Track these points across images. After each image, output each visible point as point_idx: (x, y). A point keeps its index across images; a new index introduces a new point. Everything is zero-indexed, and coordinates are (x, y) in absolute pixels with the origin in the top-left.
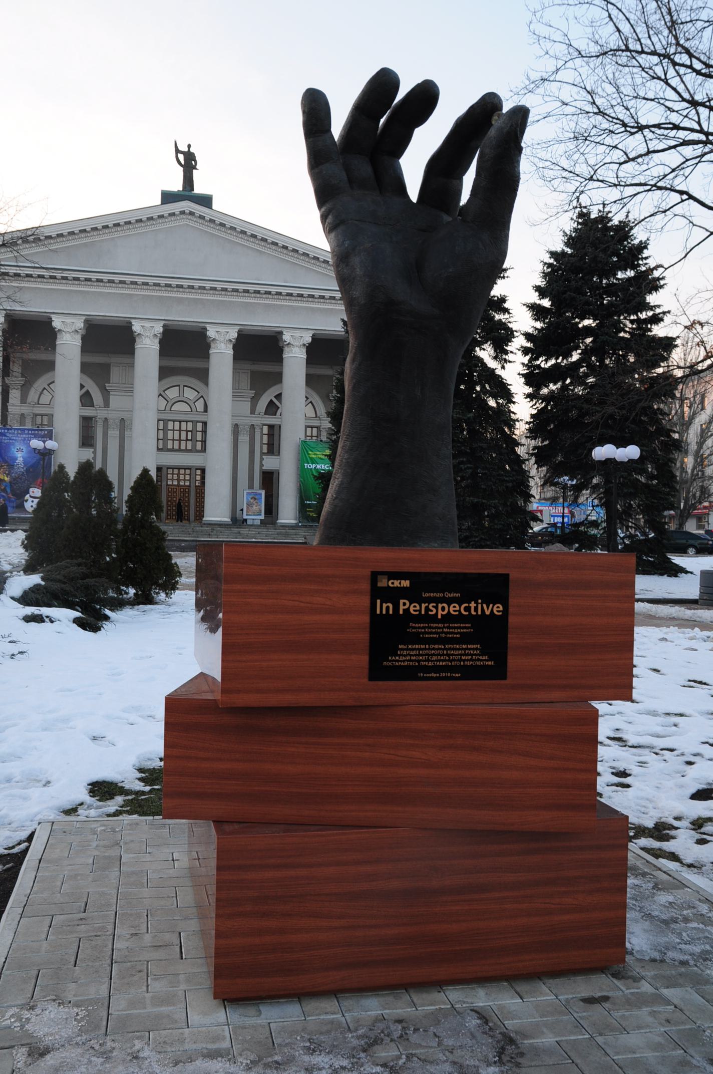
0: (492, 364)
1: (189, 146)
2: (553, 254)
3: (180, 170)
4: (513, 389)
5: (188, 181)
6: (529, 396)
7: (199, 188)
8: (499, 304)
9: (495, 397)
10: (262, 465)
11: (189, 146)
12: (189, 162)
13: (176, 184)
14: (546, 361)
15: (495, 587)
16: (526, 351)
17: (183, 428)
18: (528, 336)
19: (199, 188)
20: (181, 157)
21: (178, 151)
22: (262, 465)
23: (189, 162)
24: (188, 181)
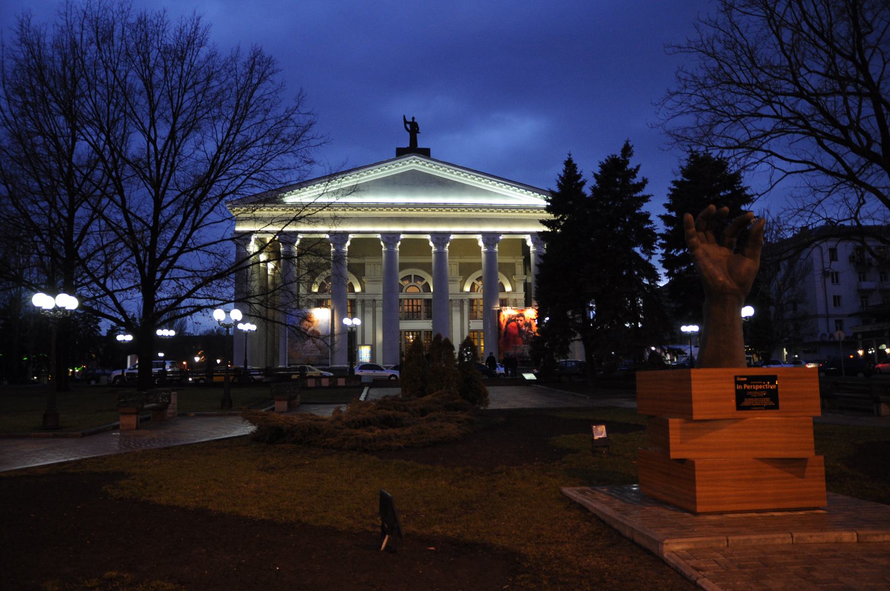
0: (645, 257)
1: (413, 118)
2: (675, 183)
3: (408, 135)
4: (658, 272)
5: (413, 141)
6: (666, 275)
7: (421, 145)
8: (645, 217)
9: (648, 278)
10: (469, 327)
11: (413, 118)
13: (406, 144)
14: (677, 251)
15: (772, 379)
16: (662, 246)
17: (415, 303)
18: (663, 236)
19: (421, 145)
20: (408, 126)
21: (406, 122)
22: (469, 327)
24: (413, 141)
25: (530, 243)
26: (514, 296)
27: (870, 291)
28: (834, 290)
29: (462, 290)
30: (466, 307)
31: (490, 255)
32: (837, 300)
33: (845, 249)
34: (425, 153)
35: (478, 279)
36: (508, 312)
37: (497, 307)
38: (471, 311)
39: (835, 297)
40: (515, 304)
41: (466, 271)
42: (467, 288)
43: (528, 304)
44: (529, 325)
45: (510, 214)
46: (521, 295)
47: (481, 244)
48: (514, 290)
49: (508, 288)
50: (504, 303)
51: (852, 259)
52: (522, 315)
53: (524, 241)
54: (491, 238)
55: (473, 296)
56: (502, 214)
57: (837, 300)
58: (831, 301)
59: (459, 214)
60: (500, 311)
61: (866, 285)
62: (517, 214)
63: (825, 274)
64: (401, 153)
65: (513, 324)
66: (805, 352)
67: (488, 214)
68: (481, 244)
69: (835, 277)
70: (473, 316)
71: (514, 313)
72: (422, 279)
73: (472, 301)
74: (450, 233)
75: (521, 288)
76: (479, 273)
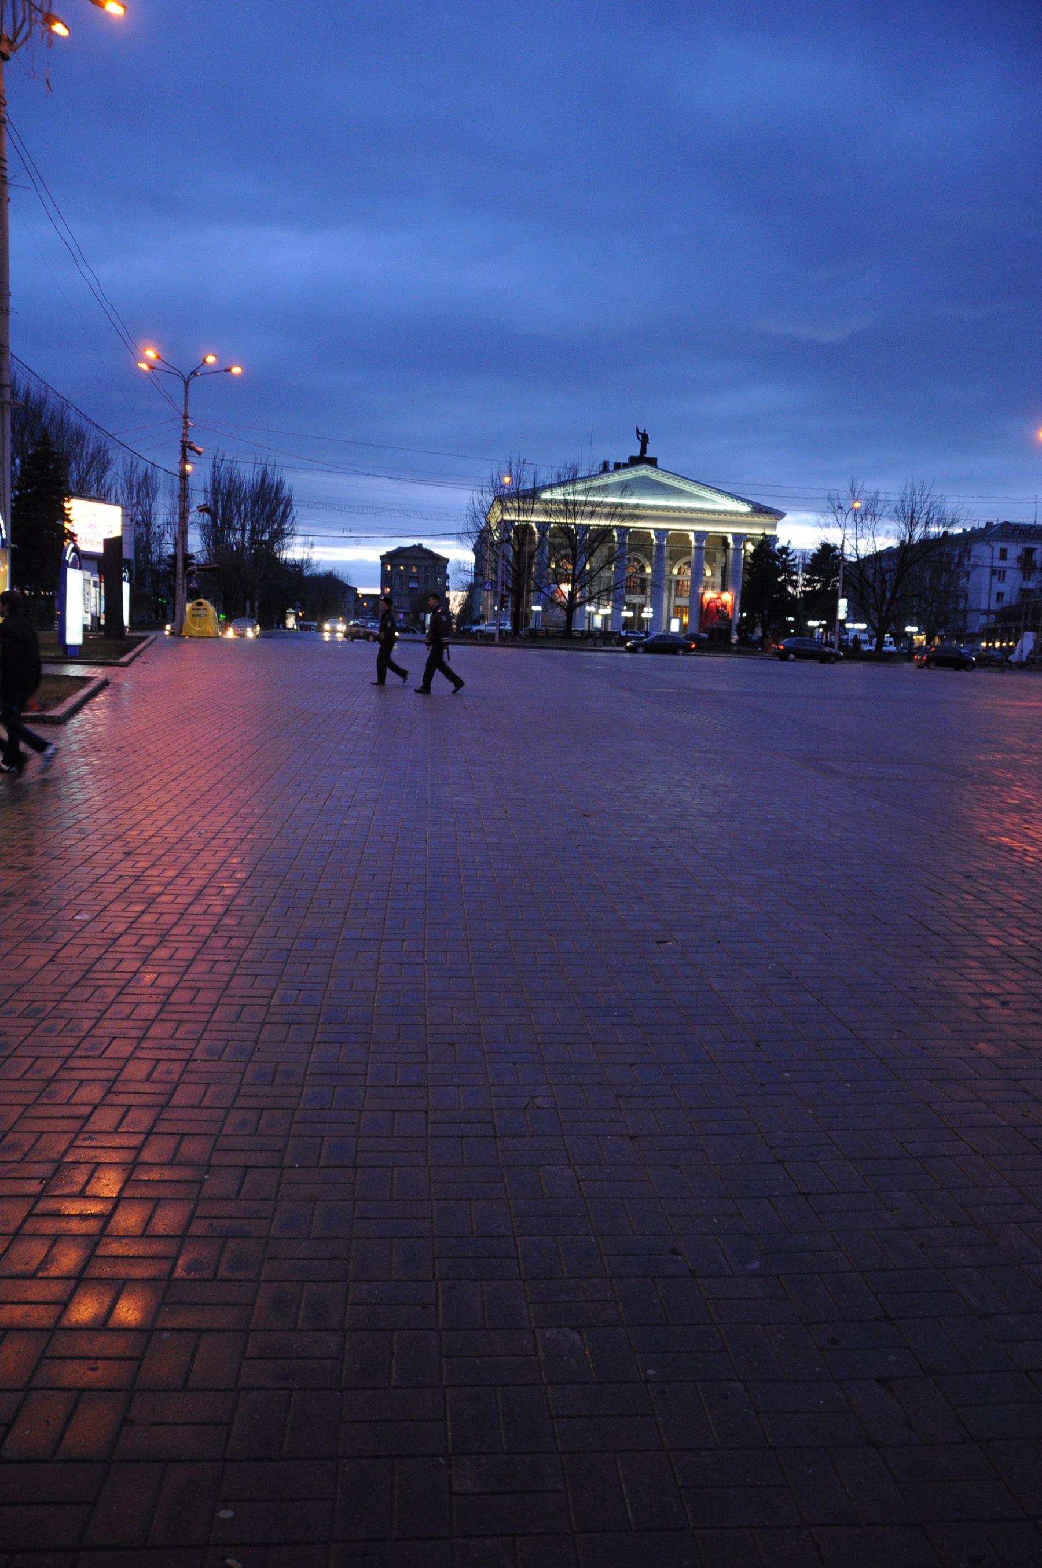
5: (643, 450)
7: (649, 454)
12: (644, 439)
13: (637, 453)
19: (649, 454)
21: (638, 432)
23: (644, 439)
24: (643, 450)
25: (730, 540)
26: (712, 580)
27: (1030, 591)
28: (999, 587)
29: (671, 572)
30: (673, 586)
31: (698, 548)
32: (1000, 596)
33: (1015, 551)
34: (653, 462)
35: (684, 564)
36: (709, 595)
37: (701, 590)
38: (677, 589)
39: (998, 594)
40: (713, 588)
41: (674, 558)
42: (675, 571)
43: (724, 589)
44: (724, 606)
45: (717, 517)
46: (718, 580)
47: (692, 537)
48: (713, 575)
49: (708, 573)
50: (706, 588)
51: (1019, 559)
52: (719, 598)
53: (725, 539)
54: (700, 536)
55: (680, 578)
56: (711, 516)
57: (1000, 596)
58: (994, 597)
59: (677, 514)
60: (703, 594)
61: (1031, 585)
62: (722, 517)
63: (994, 572)
64: (635, 462)
65: (713, 604)
66: (968, 642)
67: (700, 516)
68: (692, 537)
69: (999, 574)
70: (678, 595)
71: (715, 596)
72: (639, 562)
73: (678, 582)
74: (669, 530)
75: (719, 573)
76: (685, 559)
